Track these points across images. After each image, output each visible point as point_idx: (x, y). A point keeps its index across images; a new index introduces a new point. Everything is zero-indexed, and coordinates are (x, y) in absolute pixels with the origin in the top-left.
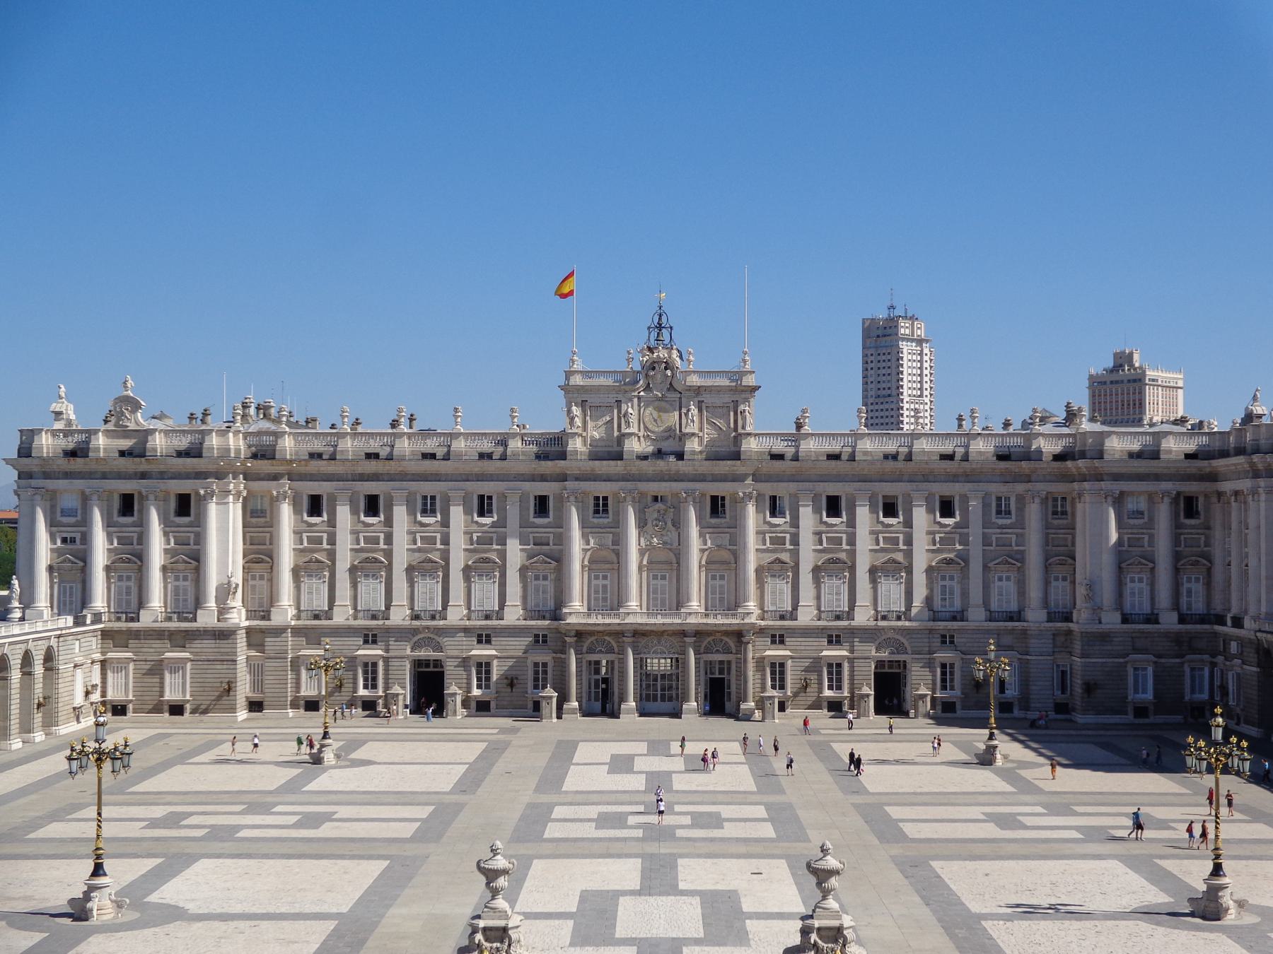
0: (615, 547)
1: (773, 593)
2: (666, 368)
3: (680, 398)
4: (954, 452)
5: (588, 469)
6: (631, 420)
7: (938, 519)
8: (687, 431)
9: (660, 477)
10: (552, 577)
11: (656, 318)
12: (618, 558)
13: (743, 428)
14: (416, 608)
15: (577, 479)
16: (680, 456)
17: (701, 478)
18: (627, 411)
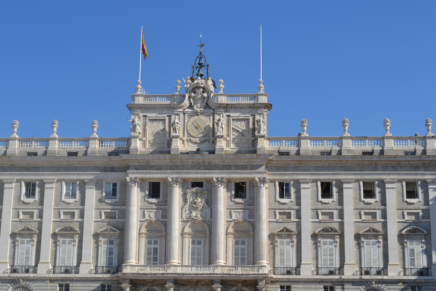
0: (165, 220)
1: (282, 254)
2: (203, 92)
3: (214, 114)
4: (415, 150)
5: (145, 161)
6: (177, 127)
7: (406, 199)
8: (218, 134)
9: (198, 167)
10: (116, 242)
11: (198, 59)
12: (166, 228)
13: (259, 132)
14: (15, 264)
15: (136, 169)
16: (213, 152)
17: (227, 167)
18: (174, 122)
